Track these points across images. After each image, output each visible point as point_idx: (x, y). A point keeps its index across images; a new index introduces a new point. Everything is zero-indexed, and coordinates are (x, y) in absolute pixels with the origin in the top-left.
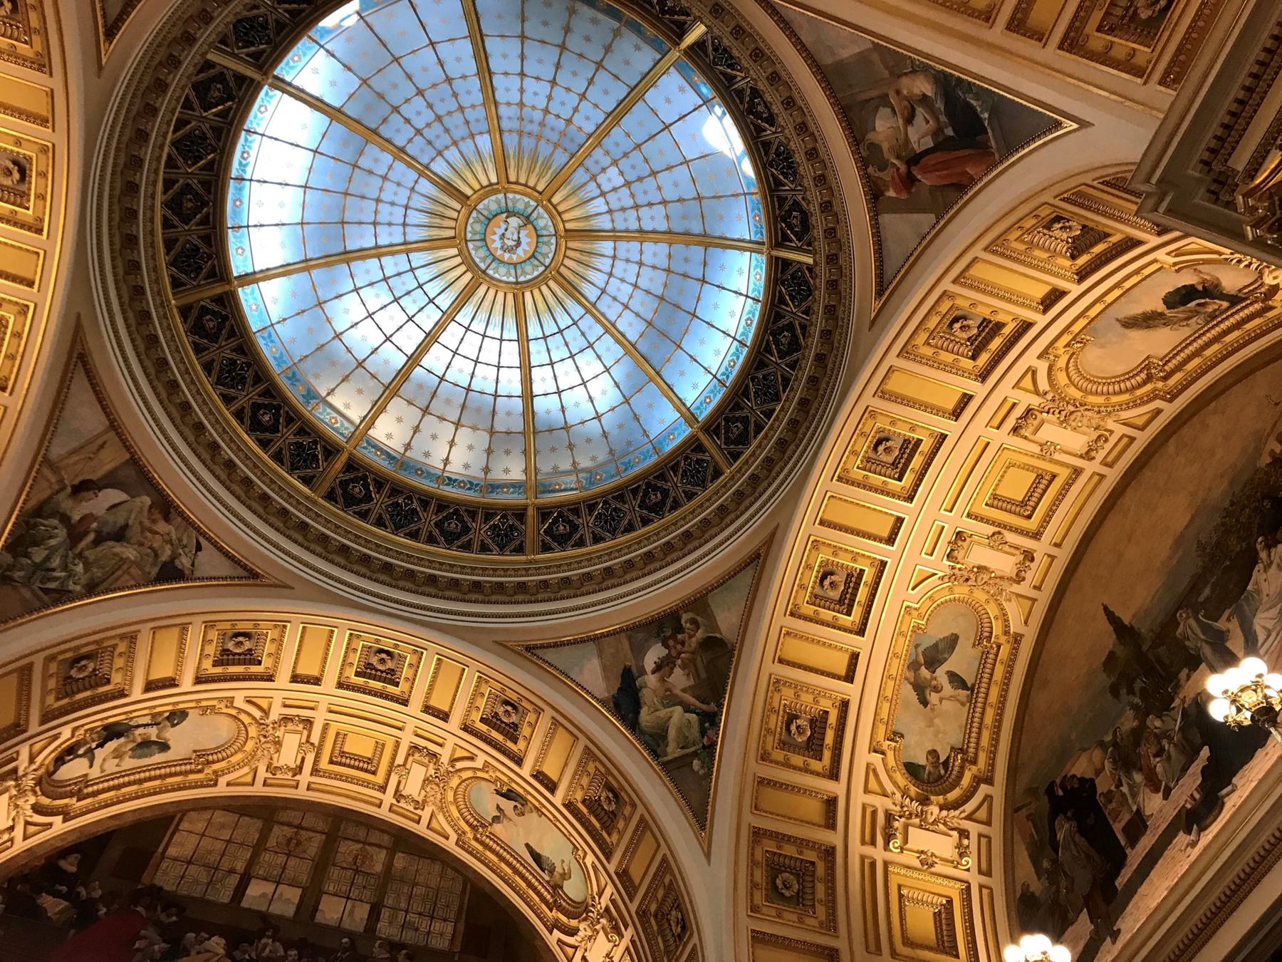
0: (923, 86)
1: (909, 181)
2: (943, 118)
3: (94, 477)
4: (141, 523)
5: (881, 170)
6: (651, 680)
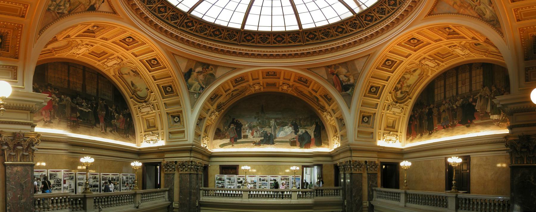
0: (352, 81)
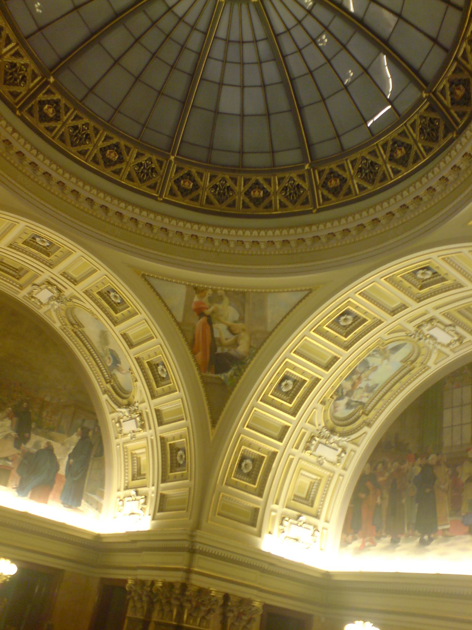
1: (200, 312)
2: (226, 350)
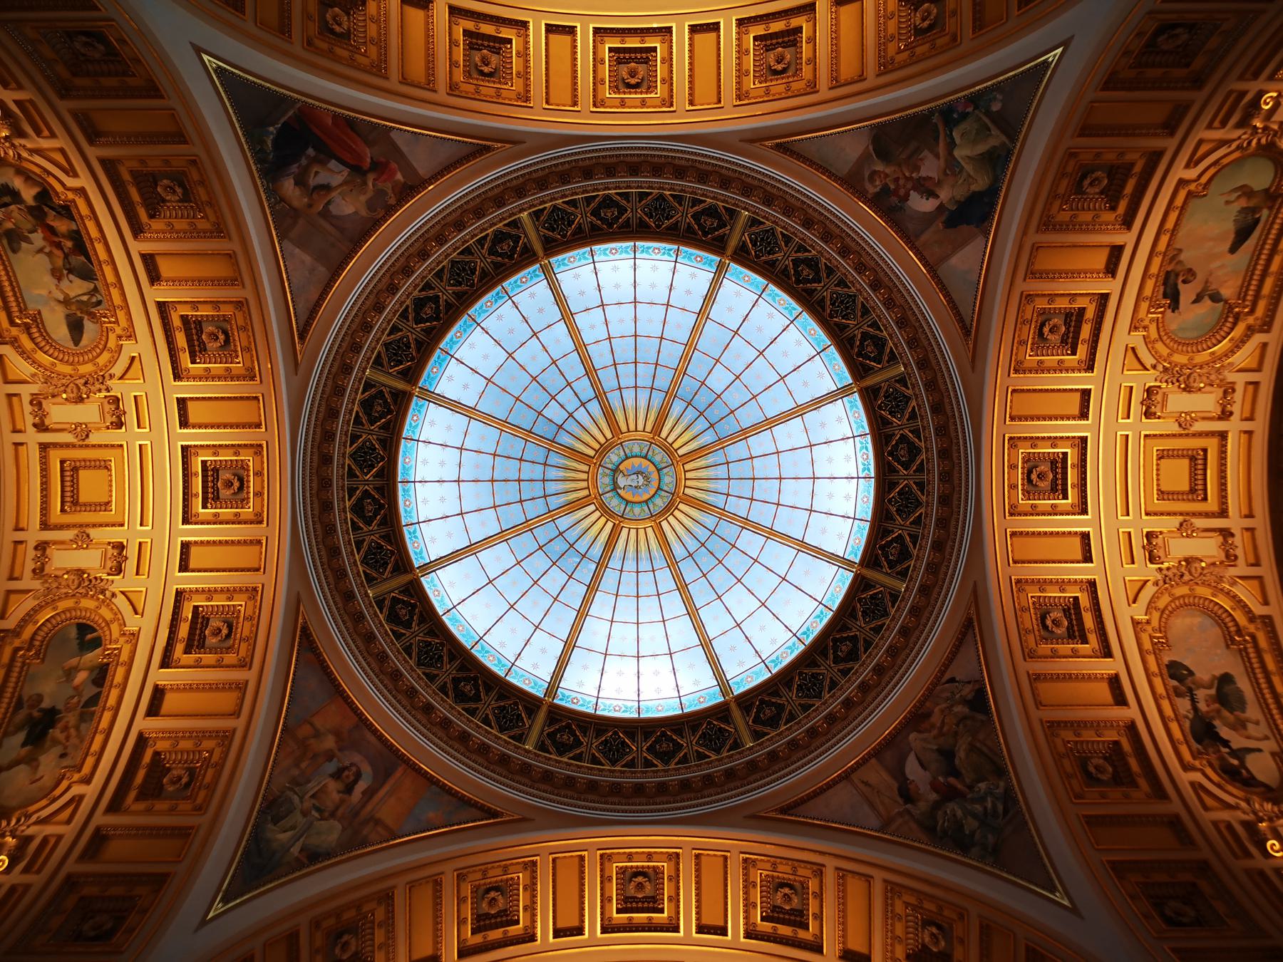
0: (288, 186)
2: (304, 162)
3: (896, 785)
4: (935, 738)
5: (386, 194)
6: (945, 194)
